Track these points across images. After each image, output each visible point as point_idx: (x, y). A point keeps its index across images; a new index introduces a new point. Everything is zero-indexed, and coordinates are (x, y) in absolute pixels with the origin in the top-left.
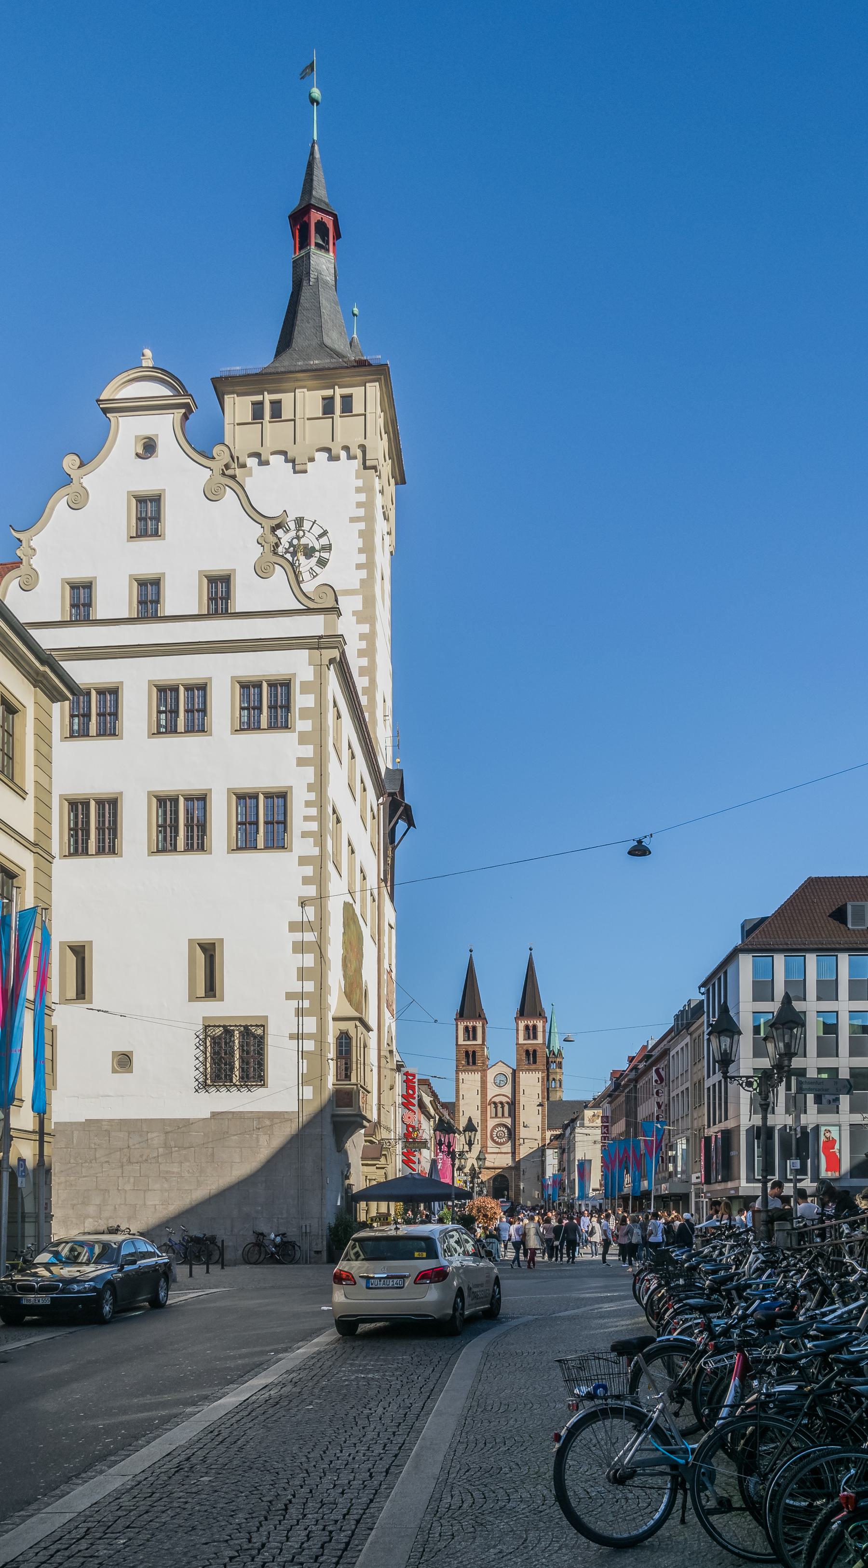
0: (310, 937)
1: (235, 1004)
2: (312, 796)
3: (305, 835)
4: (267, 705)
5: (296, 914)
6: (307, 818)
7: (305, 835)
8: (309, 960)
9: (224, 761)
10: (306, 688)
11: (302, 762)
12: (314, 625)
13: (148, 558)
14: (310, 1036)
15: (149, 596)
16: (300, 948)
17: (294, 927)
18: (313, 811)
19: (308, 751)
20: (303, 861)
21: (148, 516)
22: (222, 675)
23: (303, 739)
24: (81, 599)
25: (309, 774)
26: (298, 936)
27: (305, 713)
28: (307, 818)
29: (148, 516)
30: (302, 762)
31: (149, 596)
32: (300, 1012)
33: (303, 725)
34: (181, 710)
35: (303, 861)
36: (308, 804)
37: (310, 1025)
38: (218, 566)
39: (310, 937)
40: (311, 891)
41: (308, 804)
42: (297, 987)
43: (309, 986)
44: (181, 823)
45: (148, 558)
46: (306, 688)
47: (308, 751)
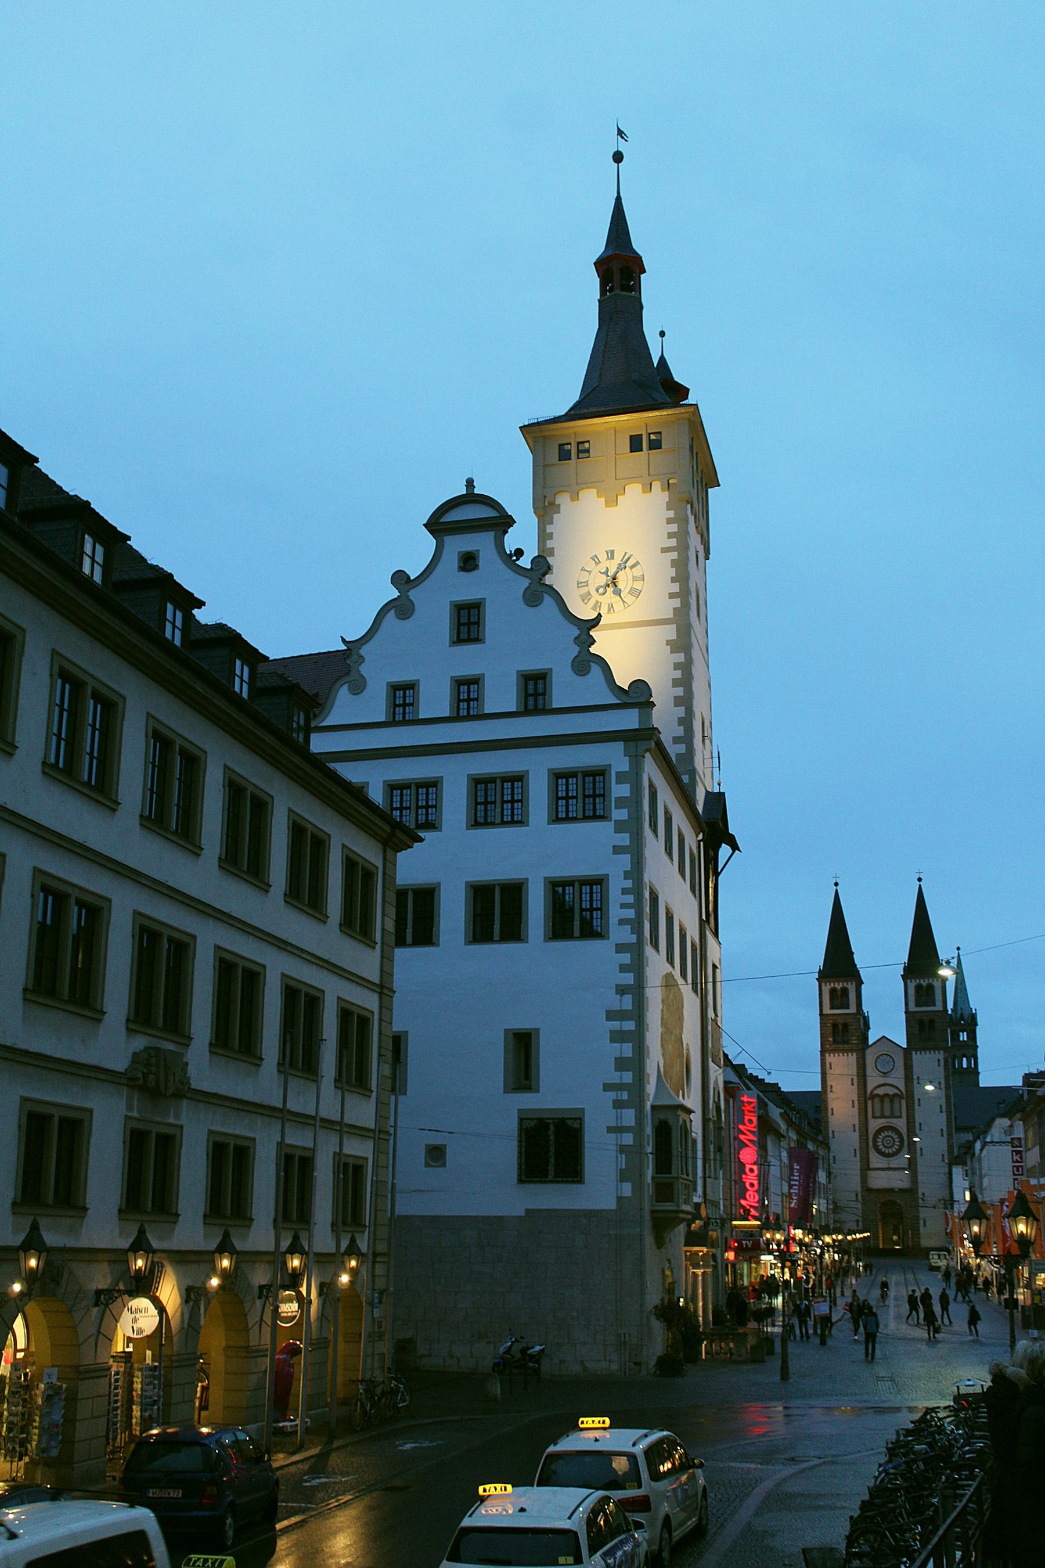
0: (630, 1025)
1: (551, 1096)
2: (629, 884)
3: (622, 922)
4: (581, 796)
5: (614, 1001)
6: (623, 906)
7: (622, 922)
8: (627, 1050)
9: (538, 852)
10: (621, 778)
11: (617, 850)
12: (629, 720)
13: (468, 660)
15: (467, 692)
16: (617, 1037)
17: (611, 1015)
18: (630, 899)
19: (624, 839)
20: (620, 948)
21: (467, 623)
23: (620, 827)
24: (402, 698)
25: (625, 861)
26: (616, 1025)
27: (621, 802)
28: (623, 906)
29: (467, 623)
30: (617, 850)
31: (467, 692)
32: (618, 1104)
33: (620, 814)
34: (496, 802)
35: (620, 948)
36: (625, 891)
37: (629, 1117)
39: (630, 1025)
40: (629, 978)
41: (625, 891)
42: (615, 1077)
43: (628, 1077)
44: (496, 912)
45: (468, 660)
46: (621, 778)
47: (624, 839)
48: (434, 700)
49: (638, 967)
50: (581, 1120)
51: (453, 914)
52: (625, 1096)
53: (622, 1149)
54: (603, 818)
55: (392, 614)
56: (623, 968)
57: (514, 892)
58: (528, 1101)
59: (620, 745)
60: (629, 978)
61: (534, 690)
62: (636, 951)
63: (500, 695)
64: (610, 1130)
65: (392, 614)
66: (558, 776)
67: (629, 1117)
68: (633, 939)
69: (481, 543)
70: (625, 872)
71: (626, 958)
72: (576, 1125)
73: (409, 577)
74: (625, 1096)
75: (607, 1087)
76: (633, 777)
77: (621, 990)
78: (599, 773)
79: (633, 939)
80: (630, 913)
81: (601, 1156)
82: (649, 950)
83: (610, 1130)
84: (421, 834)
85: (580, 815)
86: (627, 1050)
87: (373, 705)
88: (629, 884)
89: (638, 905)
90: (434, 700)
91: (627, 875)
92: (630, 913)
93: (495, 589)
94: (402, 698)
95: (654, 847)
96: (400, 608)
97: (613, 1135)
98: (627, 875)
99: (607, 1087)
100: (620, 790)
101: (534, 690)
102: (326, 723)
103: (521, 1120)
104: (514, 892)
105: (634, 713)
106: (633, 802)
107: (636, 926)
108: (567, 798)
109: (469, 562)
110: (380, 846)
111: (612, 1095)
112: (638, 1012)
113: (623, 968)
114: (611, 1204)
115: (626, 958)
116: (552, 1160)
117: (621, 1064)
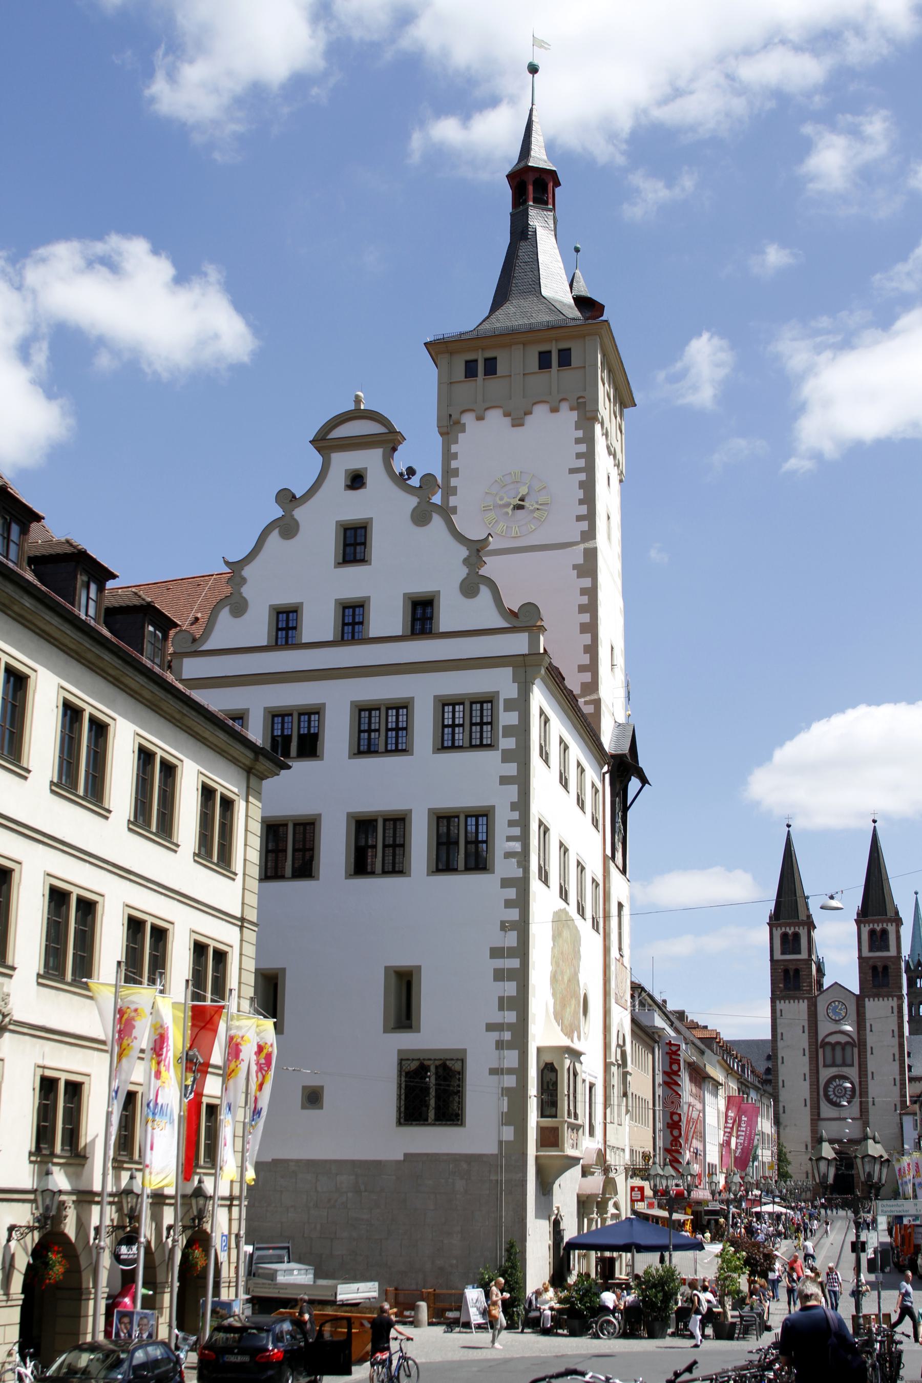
0: (515, 963)
1: (433, 1035)
2: (515, 815)
3: (508, 855)
6: (510, 839)
10: (510, 705)
11: (504, 780)
12: (518, 644)
13: (353, 582)
14: (510, 1071)
15: (352, 619)
16: (500, 975)
18: (516, 831)
19: (512, 769)
20: (506, 883)
21: (354, 544)
22: (423, 693)
23: (507, 757)
25: (512, 792)
26: (500, 963)
27: (509, 731)
29: (354, 544)
30: (504, 780)
31: (352, 619)
32: (500, 1045)
33: (506, 743)
34: (381, 732)
35: (506, 883)
36: (511, 823)
38: (421, 587)
39: (515, 963)
41: (511, 823)
44: (377, 845)
45: (353, 582)
46: (510, 705)
47: (512, 769)
48: (318, 623)
49: (522, 902)
50: (463, 1061)
51: (334, 847)
52: (507, 1036)
53: (506, 1091)
54: (490, 746)
55: (276, 533)
56: (509, 904)
57: (398, 822)
58: (407, 1041)
59: (508, 671)
60: (514, 914)
61: (422, 615)
62: (523, 885)
63: (387, 617)
64: (494, 1072)
65: (276, 533)
66: (445, 703)
67: (511, 1058)
68: (519, 873)
69: (369, 460)
70: (512, 803)
71: (511, 893)
72: (457, 1067)
73: (294, 496)
74: (507, 1036)
75: (490, 1027)
76: (522, 704)
77: (504, 926)
78: (487, 701)
79: (519, 873)
80: (517, 846)
81: (481, 1096)
82: (535, 884)
83: (494, 1072)
84: (290, 764)
85: (467, 744)
86: (510, 989)
87: (255, 627)
88: (515, 815)
89: (524, 838)
90: (318, 623)
91: (514, 807)
92: (517, 846)
93: (384, 507)
94: (286, 624)
95: (543, 778)
96: (287, 527)
97: (495, 1077)
98: (514, 807)
99: (490, 1027)
100: (508, 718)
101: (422, 615)
102: (204, 648)
103: (401, 1062)
104: (398, 822)
105: (524, 637)
106: (522, 731)
107: (523, 858)
108: (453, 726)
109: (356, 481)
110: (245, 774)
111: (495, 1036)
112: (522, 950)
113: (509, 904)
114: (493, 1149)
115: (511, 893)
116: (432, 1102)
117: (503, 1003)
